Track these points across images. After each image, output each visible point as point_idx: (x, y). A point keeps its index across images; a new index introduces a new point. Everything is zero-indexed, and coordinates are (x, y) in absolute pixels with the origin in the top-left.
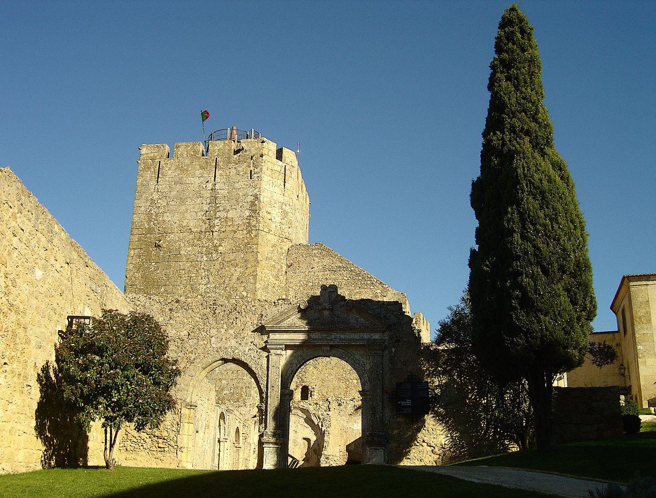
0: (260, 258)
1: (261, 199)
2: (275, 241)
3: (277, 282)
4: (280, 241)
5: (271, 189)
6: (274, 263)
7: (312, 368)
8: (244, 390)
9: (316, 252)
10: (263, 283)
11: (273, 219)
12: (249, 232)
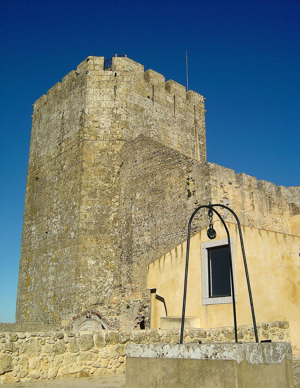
0: (85, 165)
1: (86, 112)
2: (105, 145)
3: (107, 185)
4: (111, 144)
5: (99, 99)
6: (103, 167)
8: (72, 296)
9: (138, 144)
10: (89, 189)
11: (101, 125)
12: (79, 145)
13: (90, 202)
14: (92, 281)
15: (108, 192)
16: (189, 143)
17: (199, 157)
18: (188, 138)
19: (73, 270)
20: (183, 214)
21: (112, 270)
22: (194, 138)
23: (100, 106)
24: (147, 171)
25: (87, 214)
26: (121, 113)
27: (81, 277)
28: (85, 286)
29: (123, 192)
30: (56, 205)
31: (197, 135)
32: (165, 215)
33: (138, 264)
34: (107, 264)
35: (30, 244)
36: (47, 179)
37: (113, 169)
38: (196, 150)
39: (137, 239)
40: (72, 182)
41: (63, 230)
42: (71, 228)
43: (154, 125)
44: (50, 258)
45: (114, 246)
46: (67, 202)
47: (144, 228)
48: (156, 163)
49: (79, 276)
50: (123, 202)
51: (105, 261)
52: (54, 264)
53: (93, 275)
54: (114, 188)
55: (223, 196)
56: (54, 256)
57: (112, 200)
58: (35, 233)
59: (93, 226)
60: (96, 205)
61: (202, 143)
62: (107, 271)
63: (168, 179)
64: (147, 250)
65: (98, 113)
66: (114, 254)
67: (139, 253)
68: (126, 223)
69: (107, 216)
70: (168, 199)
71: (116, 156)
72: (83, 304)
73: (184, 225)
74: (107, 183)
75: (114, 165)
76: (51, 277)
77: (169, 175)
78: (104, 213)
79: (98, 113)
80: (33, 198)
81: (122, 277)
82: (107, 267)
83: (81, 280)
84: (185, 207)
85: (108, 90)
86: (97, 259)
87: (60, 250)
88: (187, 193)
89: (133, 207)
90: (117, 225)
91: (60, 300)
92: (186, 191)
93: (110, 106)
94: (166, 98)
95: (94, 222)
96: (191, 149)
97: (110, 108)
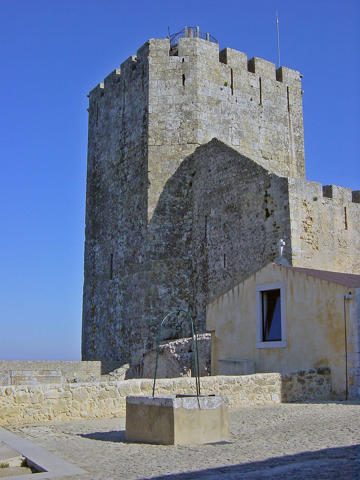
1: (150, 110)
2: (173, 151)
3: (178, 199)
4: (180, 149)
5: (164, 93)
7: (212, 294)
9: (211, 150)
13: (159, 221)
14: (164, 312)
15: (179, 208)
16: (280, 136)
17: (294, 153)
18: (279, 131)
19: (142, 300)
20: (261, 237)
21: (187, 299)
22: (287, 129)
23: (165, 103)
24: (222, 183)
25: (156, 235)
26: (192, 110)
27: (151, 308)
28: (156, 318)
29: (196, 207)
30: (120, 222)
31: (292, 125)
32: (242, 238)
33: (214, 292)
34: (180, 292)
35: (94, 267)
36: (110, 190)
37: (184, 179)
38: (289, 145)
39: (213, 264)
40: (138, 196)
41: (130, 253)
42: (139, 251)
43: (234, 119)
44: (117, 285)
45: (189, 271)
46: (133, 220)
47: (220, 252)
48: (231, 175)
49: (149, 307)
50: (197, 219)
51: (178, 289)
52: (122, 292)
53: (165, 306)
54: (187, 203)
55: (305, 216)
56: (121, 283)
57: (185, 217)
58: (98, 254)
59: (163, 248)
60: (165, 223)
61: (298, 135)
62: (180, 300)
63: (244, 195)
64: (224, 277)
65: (163, 111)
66: (188, 281)
67: (215, 280)
68: (200, 244)
69: (180, 236)
70: (245, 218)
71: (187, 164)
72: (155, 338)
73: (262, 250)
74: (177, 196)
75: (185, 174)
76: (119, 307)
77: (246, 190)
78: (175, 232)
79: (163, 111)
80: (95, 212)
81: (198, 307)
82: (181, 295)
83: (152, 311)
84: (263, 229)
85: (174, 81)
86: (168, 286)
87: (127, 276)
88: (265, 213)
89: (208, 226)
90: (191, 246)
91: (129, 333)
92: (264, 210)
93: (178, 102)
94: (249, 82)
95: (164, 243)
96: (283, 144)
97: (178, 104)
